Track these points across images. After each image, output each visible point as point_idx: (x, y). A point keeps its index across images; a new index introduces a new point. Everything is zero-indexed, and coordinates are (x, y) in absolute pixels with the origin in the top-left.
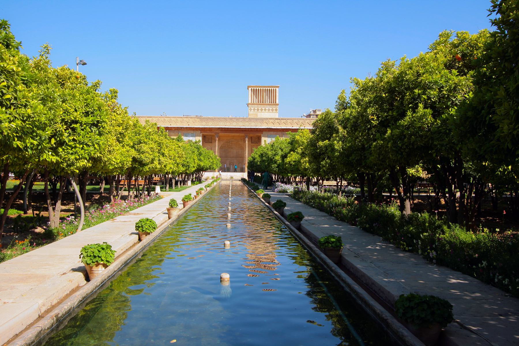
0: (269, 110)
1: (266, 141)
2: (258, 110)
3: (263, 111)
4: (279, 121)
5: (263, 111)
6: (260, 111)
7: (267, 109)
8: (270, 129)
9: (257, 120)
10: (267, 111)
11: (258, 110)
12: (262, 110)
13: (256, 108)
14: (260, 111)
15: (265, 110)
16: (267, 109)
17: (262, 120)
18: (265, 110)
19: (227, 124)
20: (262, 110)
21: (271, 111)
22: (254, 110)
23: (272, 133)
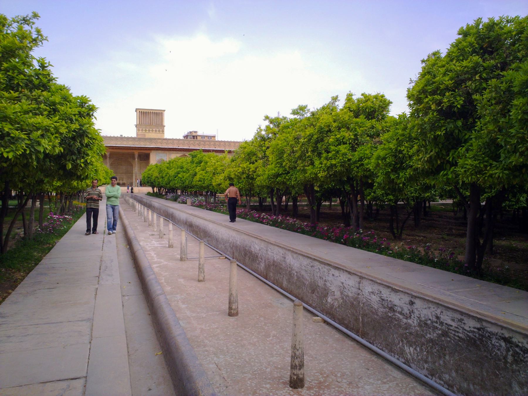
0: (156, 131)
1: (154, 159)
2: (146, 130)
3: (151, 132)
4: (166, 141)
5: (151, 132)
6: (147, 132)
7: (154, 130)
8: (158, 148)
9: (146, 139)
10: (154, 132)
11: (146, 130)
12: (149, 131)
13: (144, 129)
14: (147, 132)
15: (152, 131)
16: (154, 130)
17: (151, 140)
18: (152, 131)
19: (118, 143)
20: (149, 131)
21: (158, 132)
22: (142, 130)
23: (160, 151)
